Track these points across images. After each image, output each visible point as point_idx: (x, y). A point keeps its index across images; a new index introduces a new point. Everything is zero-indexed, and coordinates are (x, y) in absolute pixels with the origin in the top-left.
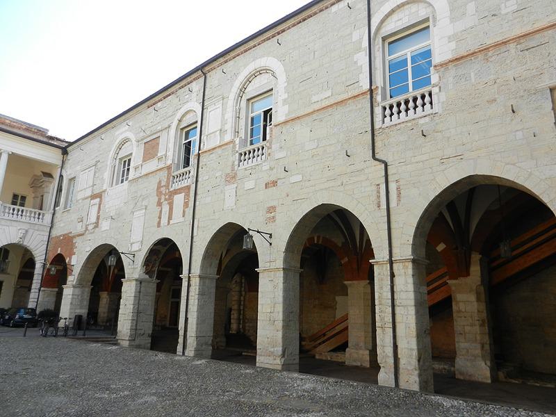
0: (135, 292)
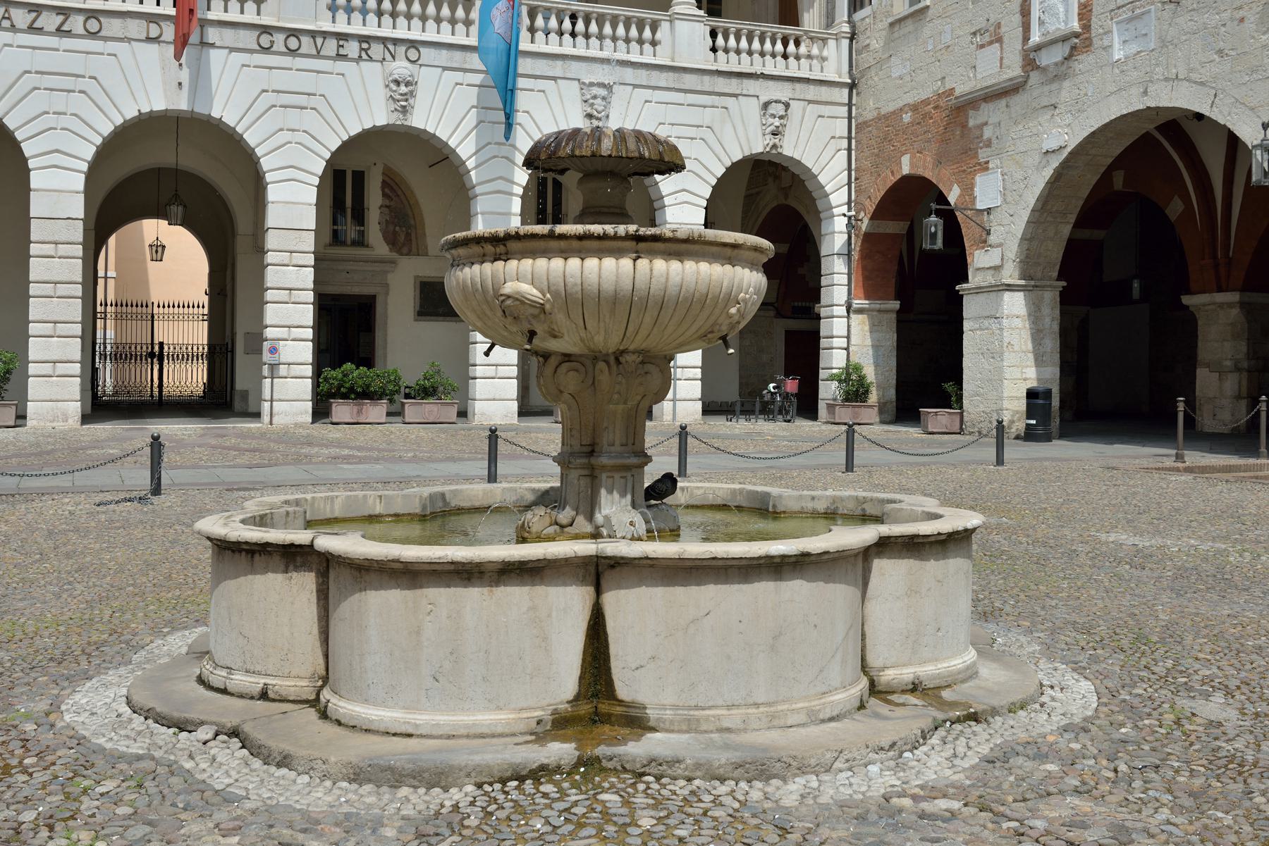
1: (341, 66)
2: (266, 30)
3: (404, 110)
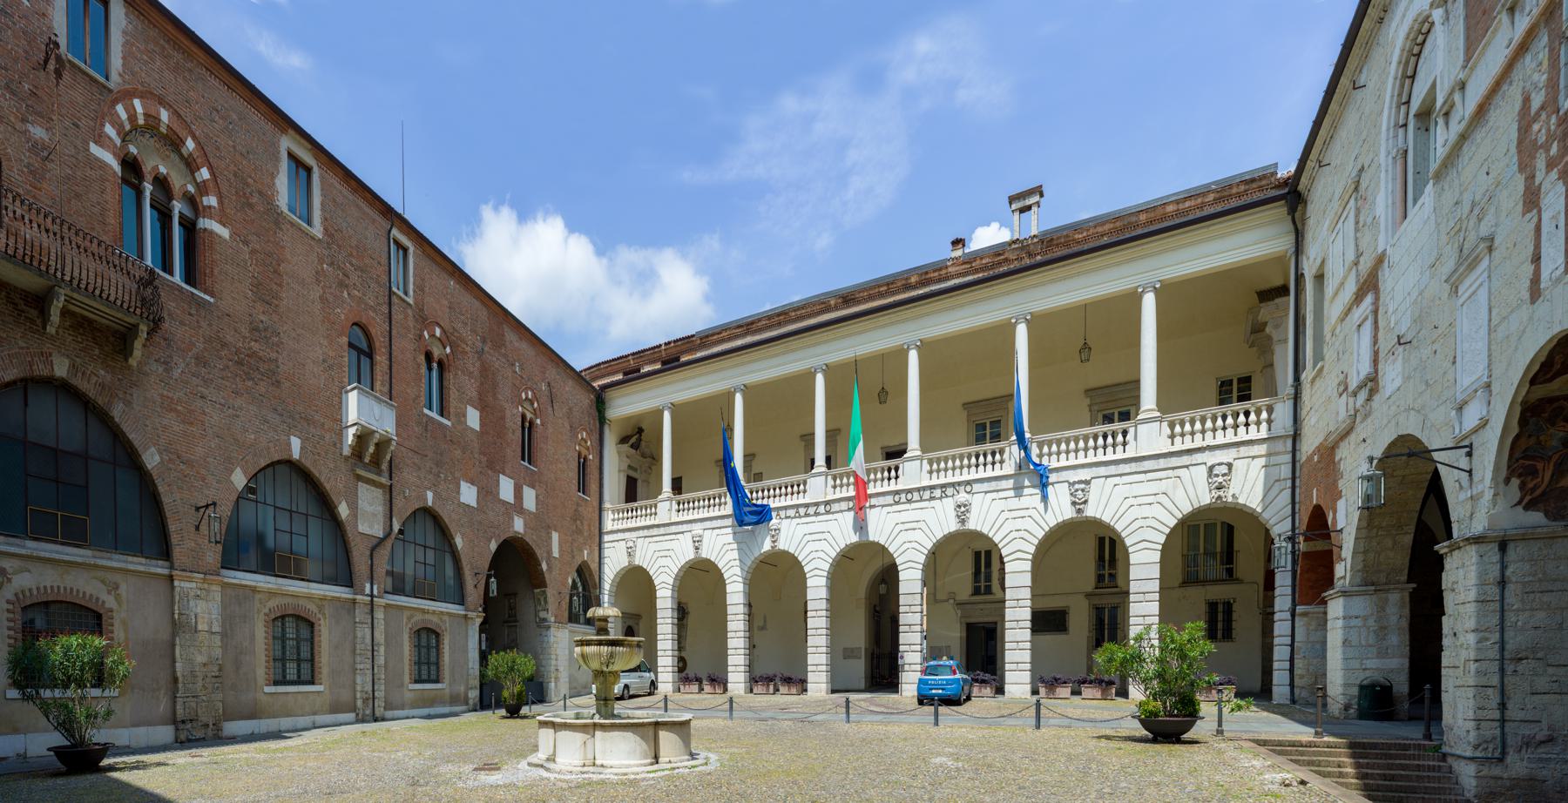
0: (1482, 584)
1: (933, 503)
2: (897, 492)
3: (963, 522)
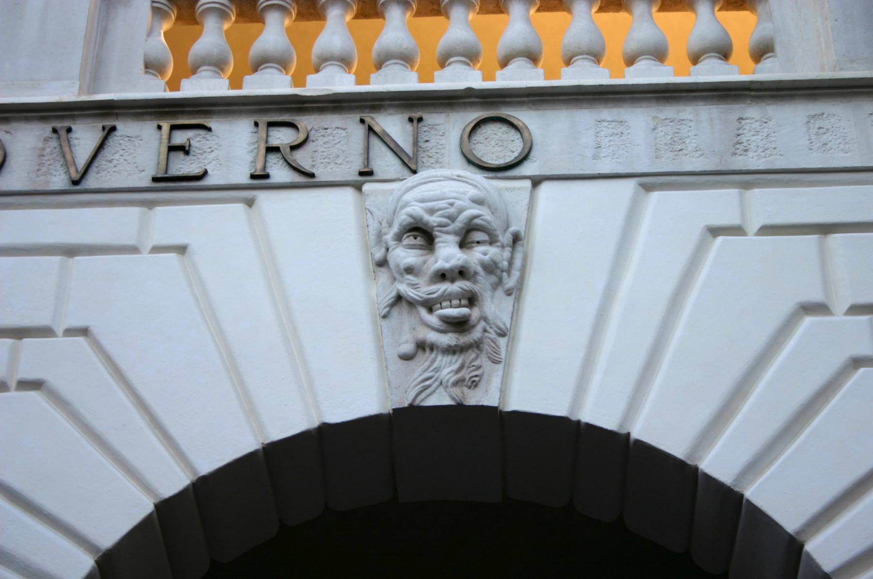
1: (175, 219)
